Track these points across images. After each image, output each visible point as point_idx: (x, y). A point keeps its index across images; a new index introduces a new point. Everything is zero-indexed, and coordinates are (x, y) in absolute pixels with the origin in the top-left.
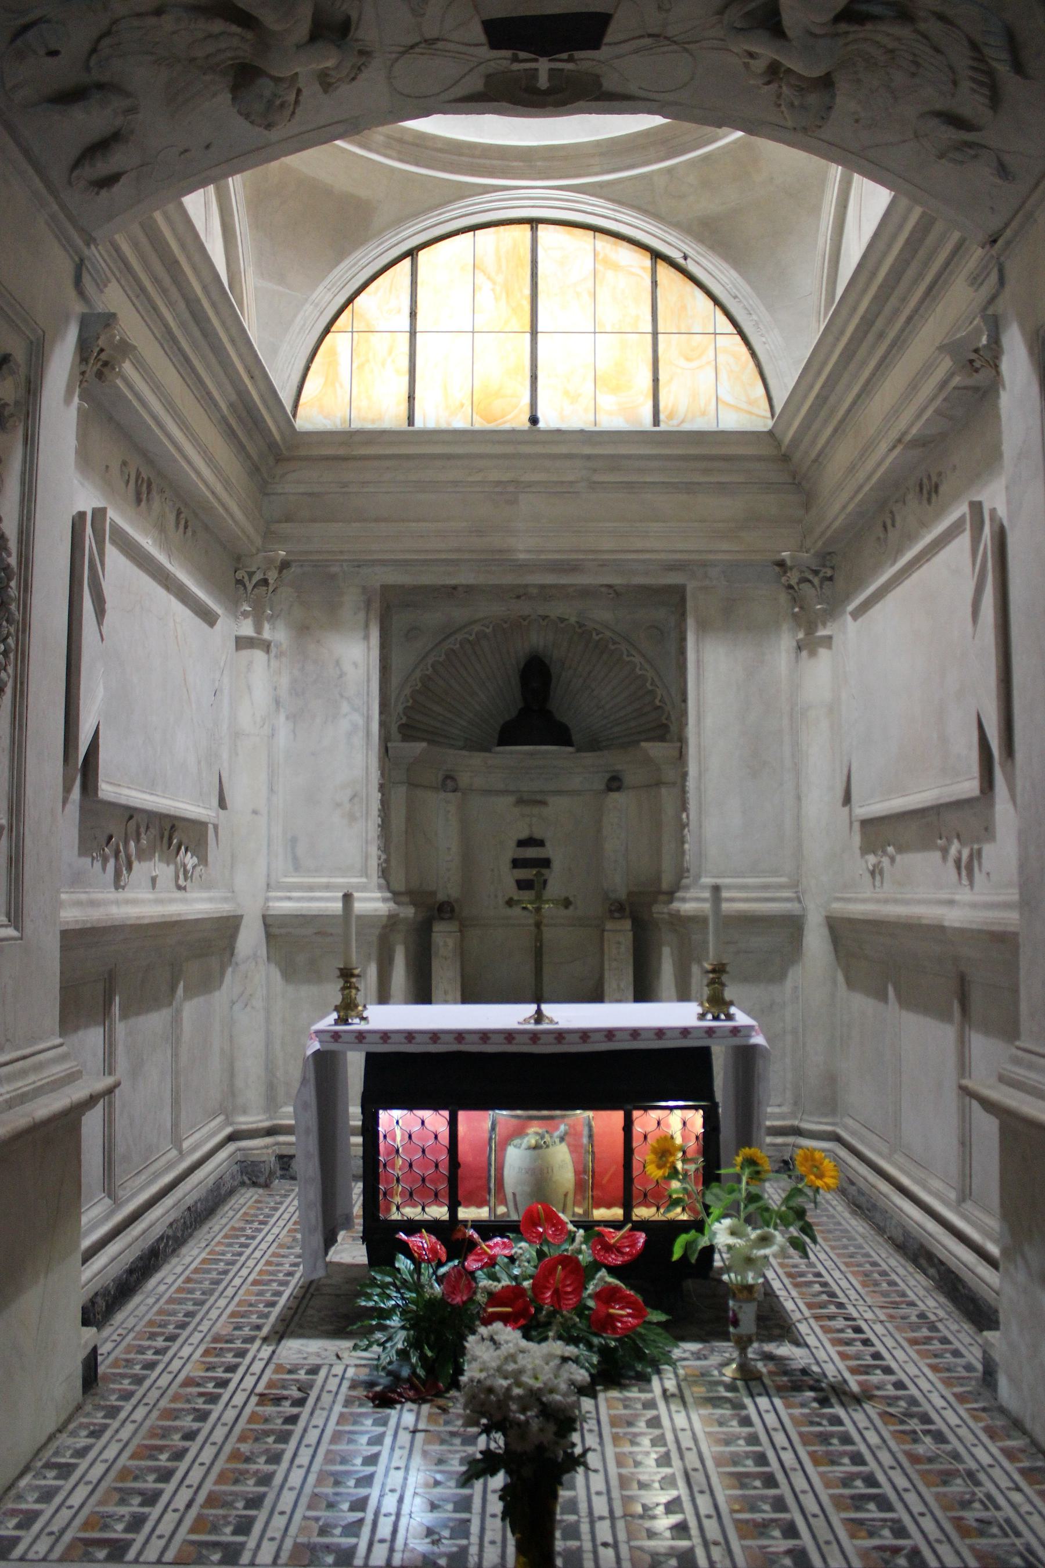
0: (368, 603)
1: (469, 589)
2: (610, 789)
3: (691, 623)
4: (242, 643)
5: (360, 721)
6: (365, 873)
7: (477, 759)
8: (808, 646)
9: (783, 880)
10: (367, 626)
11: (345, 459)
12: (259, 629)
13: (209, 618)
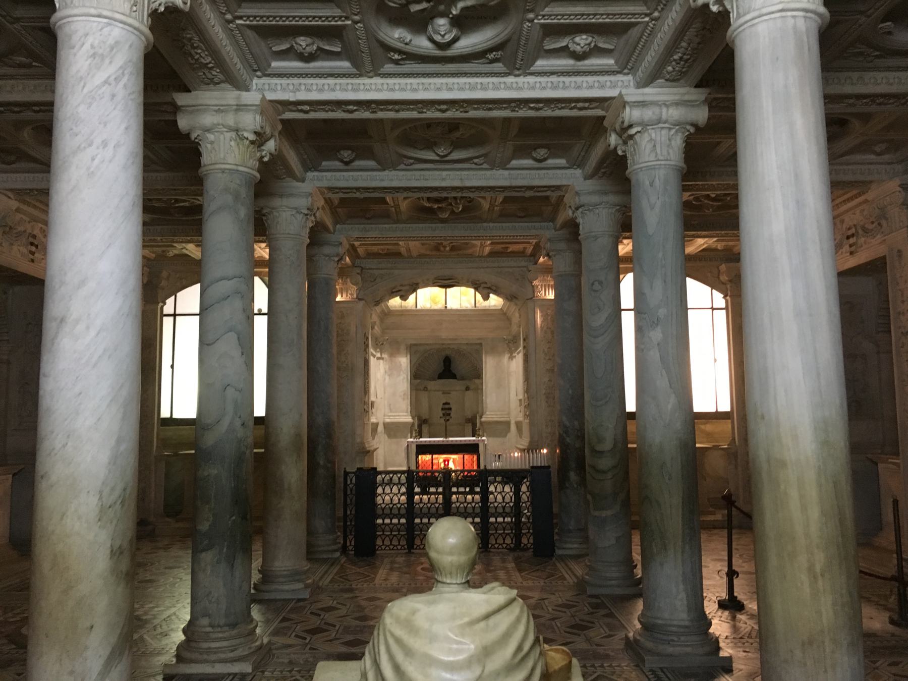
0: (407, 349)
1: (430, 344)
2: (466, 390)
3: (484, 352)
4: (378, 359)
5: (406, 376)
6: (407, 412)
7: (433, 383)
8: (511, 358)
9: (506, 413)
10: (407, 354)
11: (402, 315)
12: (381, 354)
13: (374, 356)
